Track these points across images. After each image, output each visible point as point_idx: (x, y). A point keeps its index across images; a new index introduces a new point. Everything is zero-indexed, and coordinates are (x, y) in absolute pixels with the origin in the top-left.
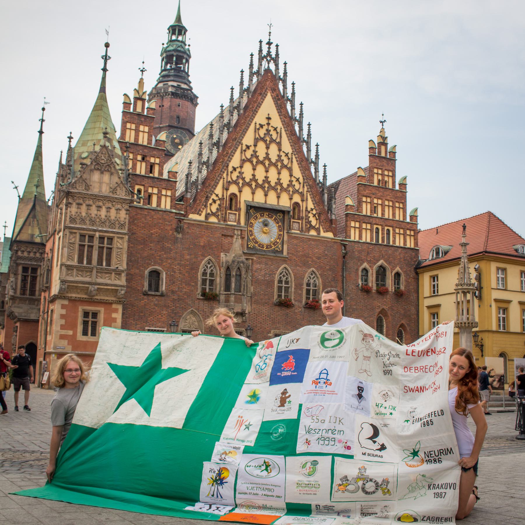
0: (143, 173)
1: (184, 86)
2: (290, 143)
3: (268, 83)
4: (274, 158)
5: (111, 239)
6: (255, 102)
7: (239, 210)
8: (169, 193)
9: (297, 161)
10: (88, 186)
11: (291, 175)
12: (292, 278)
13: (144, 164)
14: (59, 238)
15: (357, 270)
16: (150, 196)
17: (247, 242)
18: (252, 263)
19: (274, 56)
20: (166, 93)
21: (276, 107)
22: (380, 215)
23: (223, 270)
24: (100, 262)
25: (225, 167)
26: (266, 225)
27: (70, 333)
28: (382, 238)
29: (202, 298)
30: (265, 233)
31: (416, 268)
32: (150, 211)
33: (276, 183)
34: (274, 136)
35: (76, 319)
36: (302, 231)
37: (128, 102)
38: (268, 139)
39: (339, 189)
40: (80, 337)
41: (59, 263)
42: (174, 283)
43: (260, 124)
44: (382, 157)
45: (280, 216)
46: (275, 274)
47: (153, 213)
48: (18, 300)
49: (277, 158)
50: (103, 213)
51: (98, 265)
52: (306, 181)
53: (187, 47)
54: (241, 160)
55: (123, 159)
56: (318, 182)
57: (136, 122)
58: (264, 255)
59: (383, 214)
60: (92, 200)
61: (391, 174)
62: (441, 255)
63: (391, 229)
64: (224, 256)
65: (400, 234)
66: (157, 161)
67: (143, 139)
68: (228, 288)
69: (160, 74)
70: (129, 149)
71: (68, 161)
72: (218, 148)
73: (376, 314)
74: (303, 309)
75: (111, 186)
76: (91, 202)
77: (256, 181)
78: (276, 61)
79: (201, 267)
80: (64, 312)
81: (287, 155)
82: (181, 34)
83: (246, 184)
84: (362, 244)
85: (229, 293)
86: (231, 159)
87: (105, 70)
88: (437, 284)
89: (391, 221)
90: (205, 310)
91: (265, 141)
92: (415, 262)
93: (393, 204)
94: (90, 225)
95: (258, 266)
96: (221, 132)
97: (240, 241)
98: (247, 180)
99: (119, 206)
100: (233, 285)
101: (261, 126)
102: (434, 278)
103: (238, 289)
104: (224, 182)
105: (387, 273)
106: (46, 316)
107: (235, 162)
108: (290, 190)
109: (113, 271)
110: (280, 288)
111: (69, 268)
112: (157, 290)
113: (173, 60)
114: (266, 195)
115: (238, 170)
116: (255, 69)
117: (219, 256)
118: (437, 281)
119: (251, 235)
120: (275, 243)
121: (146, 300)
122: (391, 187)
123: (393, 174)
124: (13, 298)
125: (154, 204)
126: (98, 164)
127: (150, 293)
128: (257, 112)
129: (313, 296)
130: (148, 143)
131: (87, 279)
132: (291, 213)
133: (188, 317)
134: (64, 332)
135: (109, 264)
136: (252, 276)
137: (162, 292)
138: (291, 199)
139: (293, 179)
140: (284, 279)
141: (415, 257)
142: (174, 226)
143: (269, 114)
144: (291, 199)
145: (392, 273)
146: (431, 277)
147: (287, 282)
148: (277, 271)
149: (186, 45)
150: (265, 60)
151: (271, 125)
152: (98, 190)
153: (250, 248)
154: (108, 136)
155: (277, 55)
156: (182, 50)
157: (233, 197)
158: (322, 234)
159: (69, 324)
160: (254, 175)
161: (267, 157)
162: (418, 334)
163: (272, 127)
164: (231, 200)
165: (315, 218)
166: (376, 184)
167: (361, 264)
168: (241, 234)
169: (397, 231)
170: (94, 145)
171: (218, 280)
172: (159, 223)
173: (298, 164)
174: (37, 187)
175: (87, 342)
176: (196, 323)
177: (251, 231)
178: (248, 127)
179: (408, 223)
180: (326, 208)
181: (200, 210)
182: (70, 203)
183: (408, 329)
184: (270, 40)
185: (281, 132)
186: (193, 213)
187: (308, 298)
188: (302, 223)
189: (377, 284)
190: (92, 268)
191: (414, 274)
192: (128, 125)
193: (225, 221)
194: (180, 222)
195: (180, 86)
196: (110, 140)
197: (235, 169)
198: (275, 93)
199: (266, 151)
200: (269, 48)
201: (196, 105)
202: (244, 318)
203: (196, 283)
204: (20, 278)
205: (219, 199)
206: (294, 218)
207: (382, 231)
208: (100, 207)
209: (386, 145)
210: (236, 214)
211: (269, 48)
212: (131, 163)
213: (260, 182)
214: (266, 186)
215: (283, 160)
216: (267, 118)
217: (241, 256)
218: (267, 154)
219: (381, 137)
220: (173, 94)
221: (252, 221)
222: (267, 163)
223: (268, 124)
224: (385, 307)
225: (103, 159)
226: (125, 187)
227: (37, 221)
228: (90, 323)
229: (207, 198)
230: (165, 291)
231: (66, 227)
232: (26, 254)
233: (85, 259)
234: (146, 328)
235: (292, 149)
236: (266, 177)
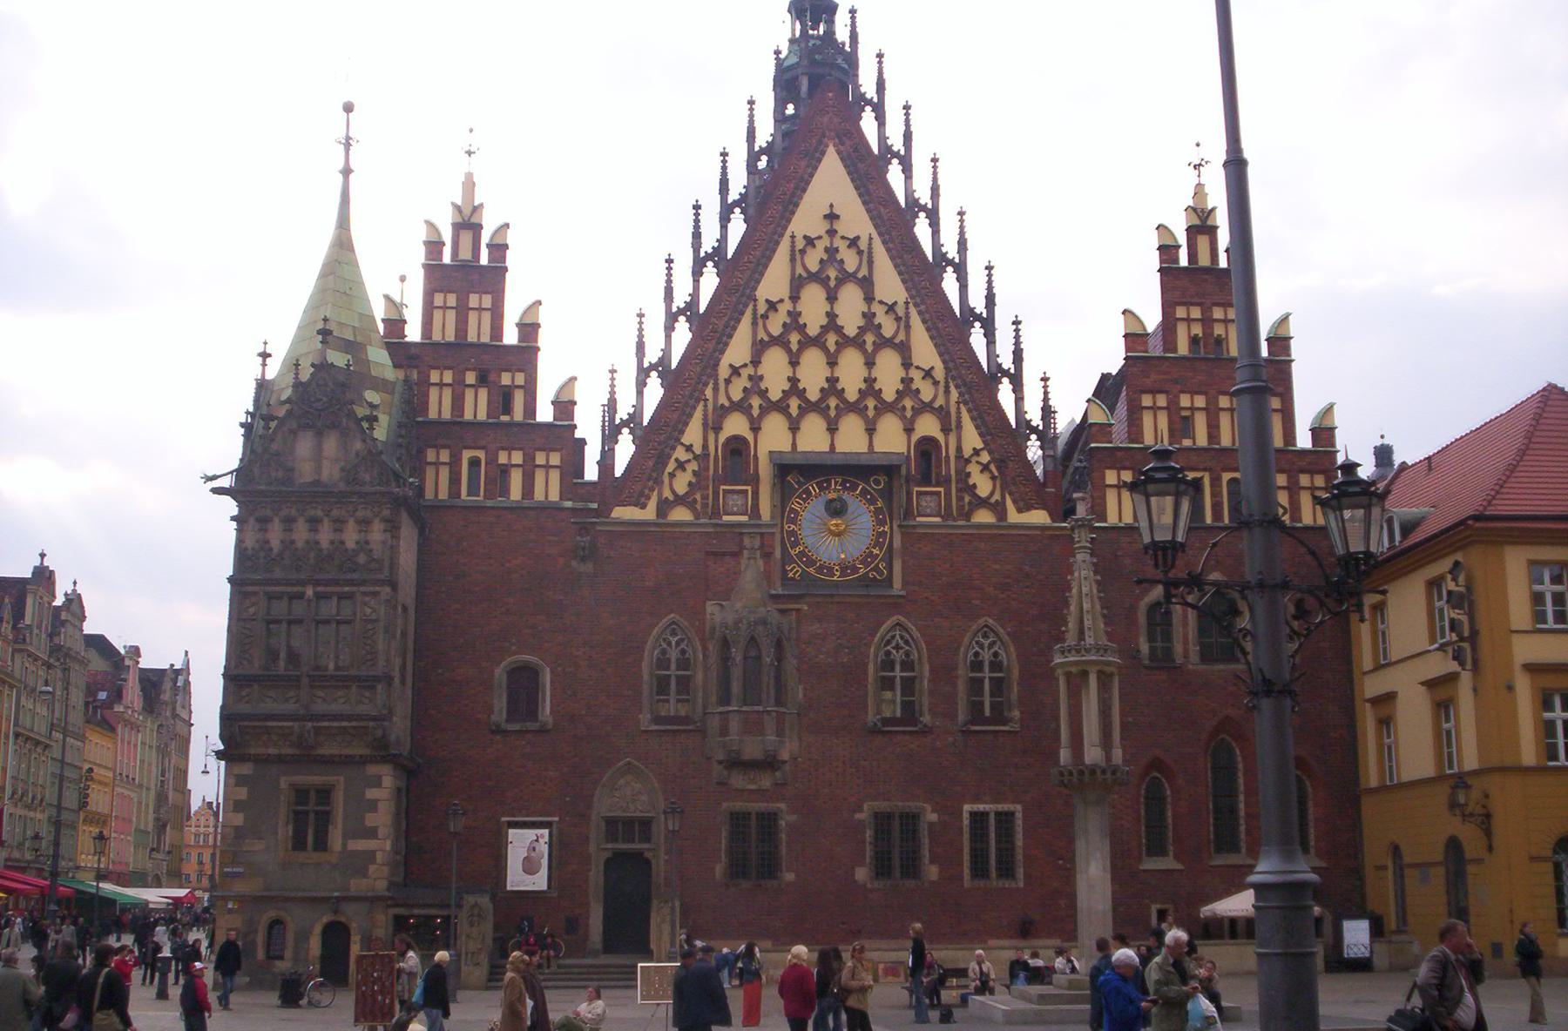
0: (482, 415)
3: (826, 120)
4: (850, 321)
7: (755, 481)
8: (555, 459)
9: (924, 321)
11: (907, 365)
13: (483, 394)
15: (1133, 609)
16: (505, 471)
17: (784, 565)
22: (1202, 440)
26: (836, 509)
34: (850, 266)
36: (947, 515)
38: (832, 273)
43: (805, 237)
45: (877, 482)
46: (868, 646)
49: (862, 323)
54: (754, 343)
58: (832, 596)
62: (1398, 537)
64: (717, 608)
77: (801, 394)
80: (243, 793)
83: (771, 407)
86: (727, 344)
87: (347, 172)
95: (816, 628)
97: (761, 562)
98: (775, 395)
100: (736, 688)
101: (810, 242)
102: (1379, 608)
104: (705, 410)
107: (738, 350)
108: (906, 404)
115: (745, 373)
119: (795, 544)
120: (867, 558)
125: (516, 493)
128: (797, 205)
129: (992, 695)
130: (492, 338)
131: (290, 707)
133: (622, 782)
138: (909, 430)
139: (914, 374)
147: (907, 665)
151: (840, 233)
157: (737, 448)
158: (1014, 517)
160: (793, 381)
161: (832, 323)
165: (986, 475)
166: (1183, 348)
168: (762, 544)
171: (700, 677)
173: (928, 330)
176: (644, 798)
178: (774, 251)
179: (1304, 452)
181: (641, 494)
188: (948, 494)
189: (1202, 644)
193: (716, 513)
197: (735, 371)
198: (848, 143)
205: (696, 457)
207: (1212, 485)
213: (813, 395)
214: (831, 404)
216: (826, 217)
218: (831, 316)
221: (796, 507)
222: (831, 340)
223: (832, 233)
228: (312, 816)
229: (662, 460)
230: (551, 720)
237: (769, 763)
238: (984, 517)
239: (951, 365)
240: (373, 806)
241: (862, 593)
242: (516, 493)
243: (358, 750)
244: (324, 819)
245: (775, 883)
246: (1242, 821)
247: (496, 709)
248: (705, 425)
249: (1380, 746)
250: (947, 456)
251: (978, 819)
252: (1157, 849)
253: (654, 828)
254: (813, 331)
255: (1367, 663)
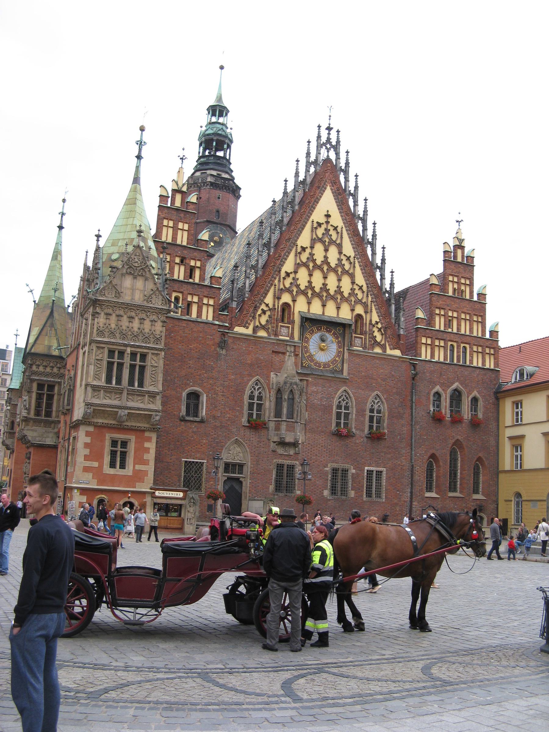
0: (182, 278)
1: (225, 176)
2: (352, 244)
3: (327, 175)
4: (333, 262)
5: (143, 357)
6: (312, 196)
7: (293, 322)
8: (211, 302)
9: (360, 266)
10: (119, 293)
11: (353, 283)
12: (353, 404)
13: (182, 268)
14: (84, 353)
15: (429, 393)
16: (189, 304)
17: (302, 360)
18: (307, 385)
19: (334, 143)
20: (204, 183)
21: (336, 202)
22: (455, 331)
23: (273, 393)
24: (131, 382)
25: (277, 272)
27: (96, 464)
28: (457, 356)
29: (248, 425)
30: (322, 350)
31: (496, 393)
32: (190, 323)
33: (335, 291)
34: (334, 237)
35: (103, 448)
37: (165, 194)
39: (407, 299)
40: (107, 470)
41: (84, 383)
42: (216, 407)
43: (317, 222)
44: (458, 263)
45: (340, 330)
46: (333, 398)
47: (192, 325)
48: (32, 422)
50: (136, 324)
51: (129, 386)
52: (370, 289)
53: (228, 131)
54: (295, 264)
55: (159, 261)
56: (384, 290)
57: (174, 218)
59: (459, 329)
60: (123, 310)
61: (468, 282)
62: (525, 377)
63: (467, 346)
64: (275, 376)
65: (478, 352)
66: (198, 264)
67: (183, 239)
68: (278, 414)
69: (197, 161)
70: (166, 251)
71: (95, 263)
72: (269, 250)
73: (450, 446)
74: (365, 440)
75: (146, 293)
76: (121, 312)
77: (313, 289)
78: (336, 148)
79: (247, 389)
80: (88, 440)
81: (348, 258)
82: (222, 116)
84: (434, 364)
85: (280, 419)
86: (284, 263)
88: (521, 412)
89: (468, 337)
90: (252, 439)
91: (323, 243)
92: (495, 385)
93: (470, 317)
94: (120, 338)
95: (314, 388)
96: (272, 232)
97: (293, 358)
98: (302, 287)
99: (154, 317)
100: (285, 411)
101: (319, 225)
102: (517, 404)
103: (291, 415)
105: (463, 398)
106: (67, 444)
107: (289, 266)
108: (351, 299)
109: (147, 393)
110: (339, 415)
111: (96, 389)
112: (196, 415)
113: (212, 146)
114: (324, 306)
115: (292, 276)
116: (313, 158)
117: (268, 376)
118: (521, 408)
120: (334, 361)
121: (183, 427)
122: (468, 297)
123: (470, 282)
124: (26, 420)
125: (194, 315)
126: (131, 267)
127: (187, 418)
128: (314, 208)
131: (116, 402)
132: (353, 327)
134: (88, 464)
135: (141, 384)
136: (307, 400)
137: (202, 418)
138: (353, 310)
140: (343, 404)
141: (495, 380)
142: (218, 340)
143: (328, 211)
144: (353, 310)
145: (468, 397)
146: (513, 402)
147: (347, 408)
148: (336, 394)
149: (227, 128)
150: (324, 147)
151: (331, 223)
152: (130, 298)
153: (305, 367)
154: (142, 234)
155: (338, 142)
156: (223, 133)
158: (389, 352)
159: (95, 454)
160: (310, 282)
161: (326, 261)
162: (498, 469)
163: (331, 225)
164: (283, 310)
165: (380, 333)
166: (450, 293)
167: (433, 388)
169: (475, 349)
170: (127, 245)
171: (267, 404)
172: (200, 337)
173: (361, 269)
174: (55, 290)
175: (115, 475)
176: (241, 455)
177: (306, 347)
178: (304, 226)
180: (393, 321)
182: (98, 313)
183: (486, 464)
184: (329, 124)
185: (342, 232)
186: (239, 325)
187: (371, 427)
189: (450, 410)
190: (122, 390)
191: (494, 400)
192: (165, 222)
193: (276, 335)
194: (224, 335)
195: (220, 175)
196: (145, 240)
197: (288, 274)
198: (335, 187)
199: (324, 254)
200: (329, 134)
201: (239, 197)
202: (297, 449)
203: (242, 407)
204: (34, 396)
205: (270, 310)
206: (355, 333)
207: (457, 348)
208: (133, 318)
209: (462, 248)
210: (288, 327)
211: (329, 134)
212: (168, 266)
213: (317, 290)
214: (324, 295)
215: (344, 265)
216: (325, 215)
217: (295, 377)
218: (326, 257)
219: (458, 238)
220: (212, 184)
221: (308, 336)
222: (325, 268)
223: (327, 222)
224: (459, 437)
225: (137, 261)
226: (162, 295)
227: (55, 330)
228: (119, 453)
229: (256, 308)
231: (92, 341)
232: (41, 369)
233: (114, 378)
234: (183, 460)
235: (355, 252)
236: (325, 285)
237: (295, 444)
238: (378, 350)
239: (369, 285)
240: (147, 450)
241: (331, 375)
242: (194, 315)
243: (143, 425)
244: (124, 455)
245: (293, 495)
246: (459, 480)
247: (182, 411)
248: (274, 296)
249: (512, 455)
250: (366, 323)
251: (370, 472)
252: (429, 489)
253: (245, 468)
254: (319, 262)
255: (508, 422)
